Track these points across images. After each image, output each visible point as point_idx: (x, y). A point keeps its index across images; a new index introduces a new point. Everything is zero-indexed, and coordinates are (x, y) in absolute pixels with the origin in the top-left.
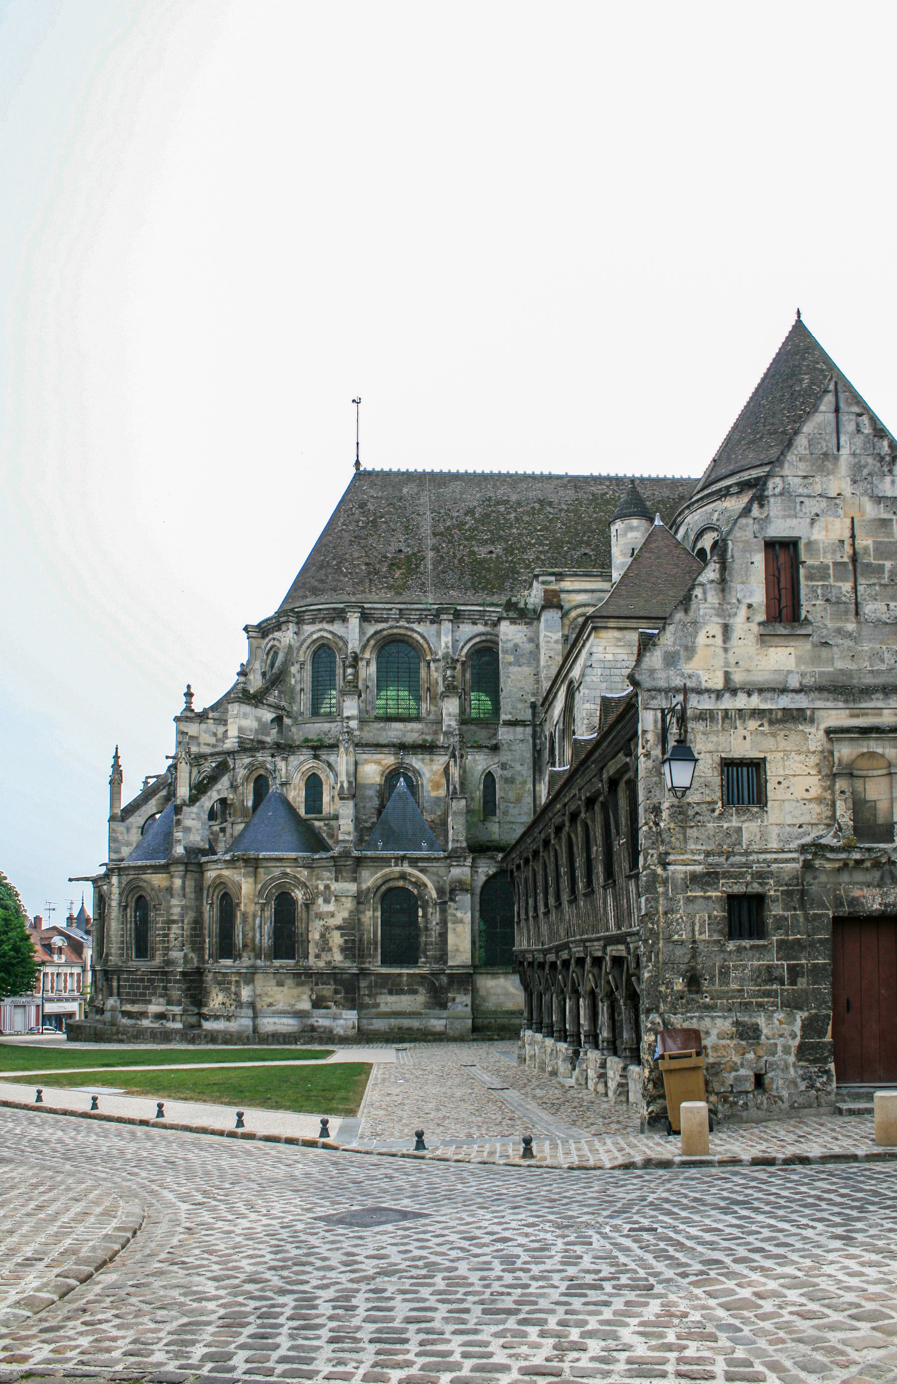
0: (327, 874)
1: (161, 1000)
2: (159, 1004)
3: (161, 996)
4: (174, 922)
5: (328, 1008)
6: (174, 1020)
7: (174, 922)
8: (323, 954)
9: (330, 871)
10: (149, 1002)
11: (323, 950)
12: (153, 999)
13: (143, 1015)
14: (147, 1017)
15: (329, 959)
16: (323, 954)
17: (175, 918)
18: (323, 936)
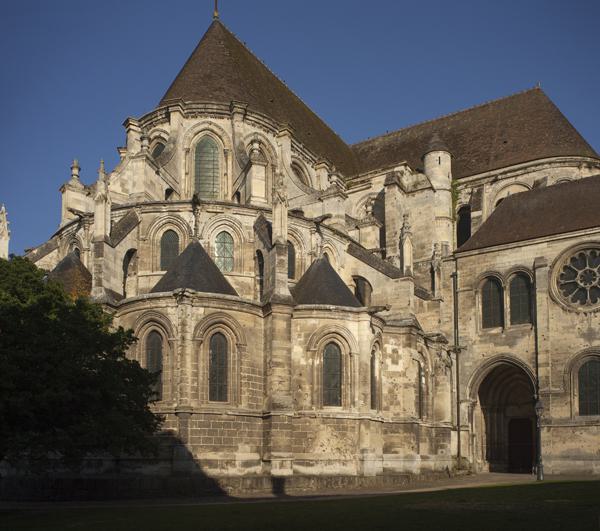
0: (392, 340)
1: (247, 447)
2: (245, 452)
3: (247, 443)
4: (278, 364)
5: (396, 452)
6: (282, 466)
7: (278, 364)
8: (392, 407)
9: (396, 337)
10: (236, 448)
11: (392, 404)
12: (240, 445)
13: (231, 463)
14: (234, 465)
15: (396, 412)
16: (392, 407)
17: (280, 360)
18: (391, 391)
